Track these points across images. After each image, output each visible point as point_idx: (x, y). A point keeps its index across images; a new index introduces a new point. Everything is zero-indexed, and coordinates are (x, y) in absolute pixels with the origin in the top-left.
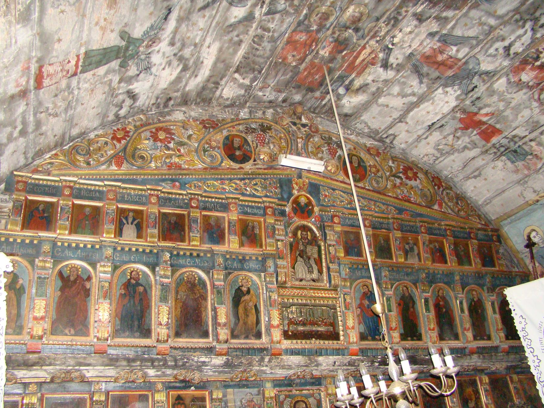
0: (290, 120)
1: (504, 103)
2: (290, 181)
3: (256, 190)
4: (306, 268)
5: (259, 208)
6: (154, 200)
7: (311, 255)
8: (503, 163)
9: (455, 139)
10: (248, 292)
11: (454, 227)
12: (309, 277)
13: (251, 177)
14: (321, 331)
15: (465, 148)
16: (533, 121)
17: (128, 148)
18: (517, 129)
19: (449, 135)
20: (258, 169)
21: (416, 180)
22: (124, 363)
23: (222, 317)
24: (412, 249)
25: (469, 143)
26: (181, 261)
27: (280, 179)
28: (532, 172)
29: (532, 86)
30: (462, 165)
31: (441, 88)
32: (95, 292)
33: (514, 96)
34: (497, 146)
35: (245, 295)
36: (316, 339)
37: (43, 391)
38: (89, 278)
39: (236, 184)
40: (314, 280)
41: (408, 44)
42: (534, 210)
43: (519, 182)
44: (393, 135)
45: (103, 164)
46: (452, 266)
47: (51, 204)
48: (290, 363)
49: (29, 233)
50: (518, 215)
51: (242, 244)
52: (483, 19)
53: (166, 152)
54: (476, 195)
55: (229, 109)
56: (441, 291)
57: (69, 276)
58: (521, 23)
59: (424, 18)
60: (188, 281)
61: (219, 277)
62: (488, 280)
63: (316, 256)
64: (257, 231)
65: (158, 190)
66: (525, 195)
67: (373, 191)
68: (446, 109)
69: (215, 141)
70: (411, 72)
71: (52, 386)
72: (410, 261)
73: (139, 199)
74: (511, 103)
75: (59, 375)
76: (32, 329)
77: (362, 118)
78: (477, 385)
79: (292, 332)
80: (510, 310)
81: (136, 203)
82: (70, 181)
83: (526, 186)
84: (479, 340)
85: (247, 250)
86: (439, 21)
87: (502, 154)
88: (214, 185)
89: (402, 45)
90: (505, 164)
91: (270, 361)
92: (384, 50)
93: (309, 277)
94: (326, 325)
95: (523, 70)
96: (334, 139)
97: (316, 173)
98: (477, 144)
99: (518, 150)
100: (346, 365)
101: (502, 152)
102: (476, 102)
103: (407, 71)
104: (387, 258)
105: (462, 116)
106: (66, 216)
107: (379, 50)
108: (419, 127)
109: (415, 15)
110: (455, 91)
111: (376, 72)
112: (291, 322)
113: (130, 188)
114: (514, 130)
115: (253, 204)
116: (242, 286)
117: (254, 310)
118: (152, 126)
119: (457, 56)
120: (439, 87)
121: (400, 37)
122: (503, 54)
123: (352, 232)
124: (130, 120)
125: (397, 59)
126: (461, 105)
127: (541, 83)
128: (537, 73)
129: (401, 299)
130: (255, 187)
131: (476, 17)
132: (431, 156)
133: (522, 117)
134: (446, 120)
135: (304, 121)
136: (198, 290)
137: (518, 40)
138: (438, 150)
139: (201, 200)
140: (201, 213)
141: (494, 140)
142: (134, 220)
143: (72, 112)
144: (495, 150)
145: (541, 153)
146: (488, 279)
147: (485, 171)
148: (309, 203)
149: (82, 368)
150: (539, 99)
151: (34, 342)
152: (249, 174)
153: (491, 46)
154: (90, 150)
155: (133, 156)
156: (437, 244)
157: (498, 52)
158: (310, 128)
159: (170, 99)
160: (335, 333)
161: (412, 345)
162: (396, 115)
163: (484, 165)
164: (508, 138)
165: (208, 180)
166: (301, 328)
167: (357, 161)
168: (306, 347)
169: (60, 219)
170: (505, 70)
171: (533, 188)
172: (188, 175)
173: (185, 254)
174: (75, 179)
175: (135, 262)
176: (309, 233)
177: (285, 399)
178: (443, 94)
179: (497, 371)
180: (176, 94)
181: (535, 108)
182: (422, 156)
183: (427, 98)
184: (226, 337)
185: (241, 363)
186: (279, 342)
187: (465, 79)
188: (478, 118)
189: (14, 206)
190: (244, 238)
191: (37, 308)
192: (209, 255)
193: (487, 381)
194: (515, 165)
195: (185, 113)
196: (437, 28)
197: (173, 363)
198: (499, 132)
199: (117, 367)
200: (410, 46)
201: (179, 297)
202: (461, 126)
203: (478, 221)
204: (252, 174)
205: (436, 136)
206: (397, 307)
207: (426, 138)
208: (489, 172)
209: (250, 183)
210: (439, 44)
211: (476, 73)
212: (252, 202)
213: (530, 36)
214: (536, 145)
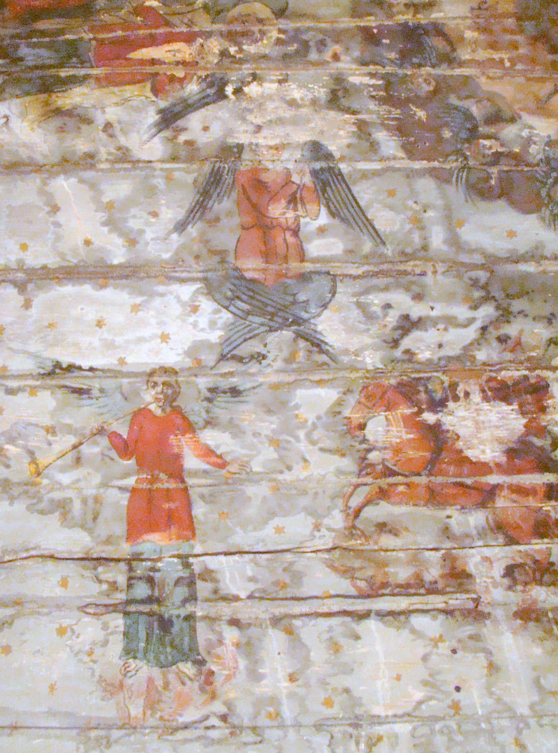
8: (100, 635)
9: (70, 458)
16: (291, 563)
18: (236, 557)
25: (85, 502)
29: (371, 465)
31: (198, 285)
33: (315, 456)
34: (140, 569)
41: (259, 121)
52: (431, 214)
58: (477, 294)
59: (345, 102)
70: (195, 181)
74: (289, 468)
86: (360, 137)
89: (250, 111)
90: (105, 643)
92: (211, 85)
95: (389, 407)
98: (101, 518)
103: (188, 172)
105: (153, 407)
107: (203, 74)
108: (34, 347)
109: (339, 79)
110: (212, 324)
111: (138, 110)
114: (226, 554)
119: (310, 241)
120: (193, 280)
121: (267, 92)
122: (387, 330)
125: (206, 129)
127: (398, 474)
128: (409, 440)
131: (423, 199)
133: (279, 530)
134: (109, 384)
137: (441, 326)
145: (228, 678)
147: (32, 621)
150: (357, 513)
153: (386, 289)
157: (386, 315)
164: (187, 565)
170: (354, 375)
178: (183, 304)
181: (329, 529)
187: (263, 315)
194: (126, 666)
196: (339, 148)
200: (259, 128)
210: (308, 180)
211: (298, 321)
213: (468, 342)
214: (237, 645)
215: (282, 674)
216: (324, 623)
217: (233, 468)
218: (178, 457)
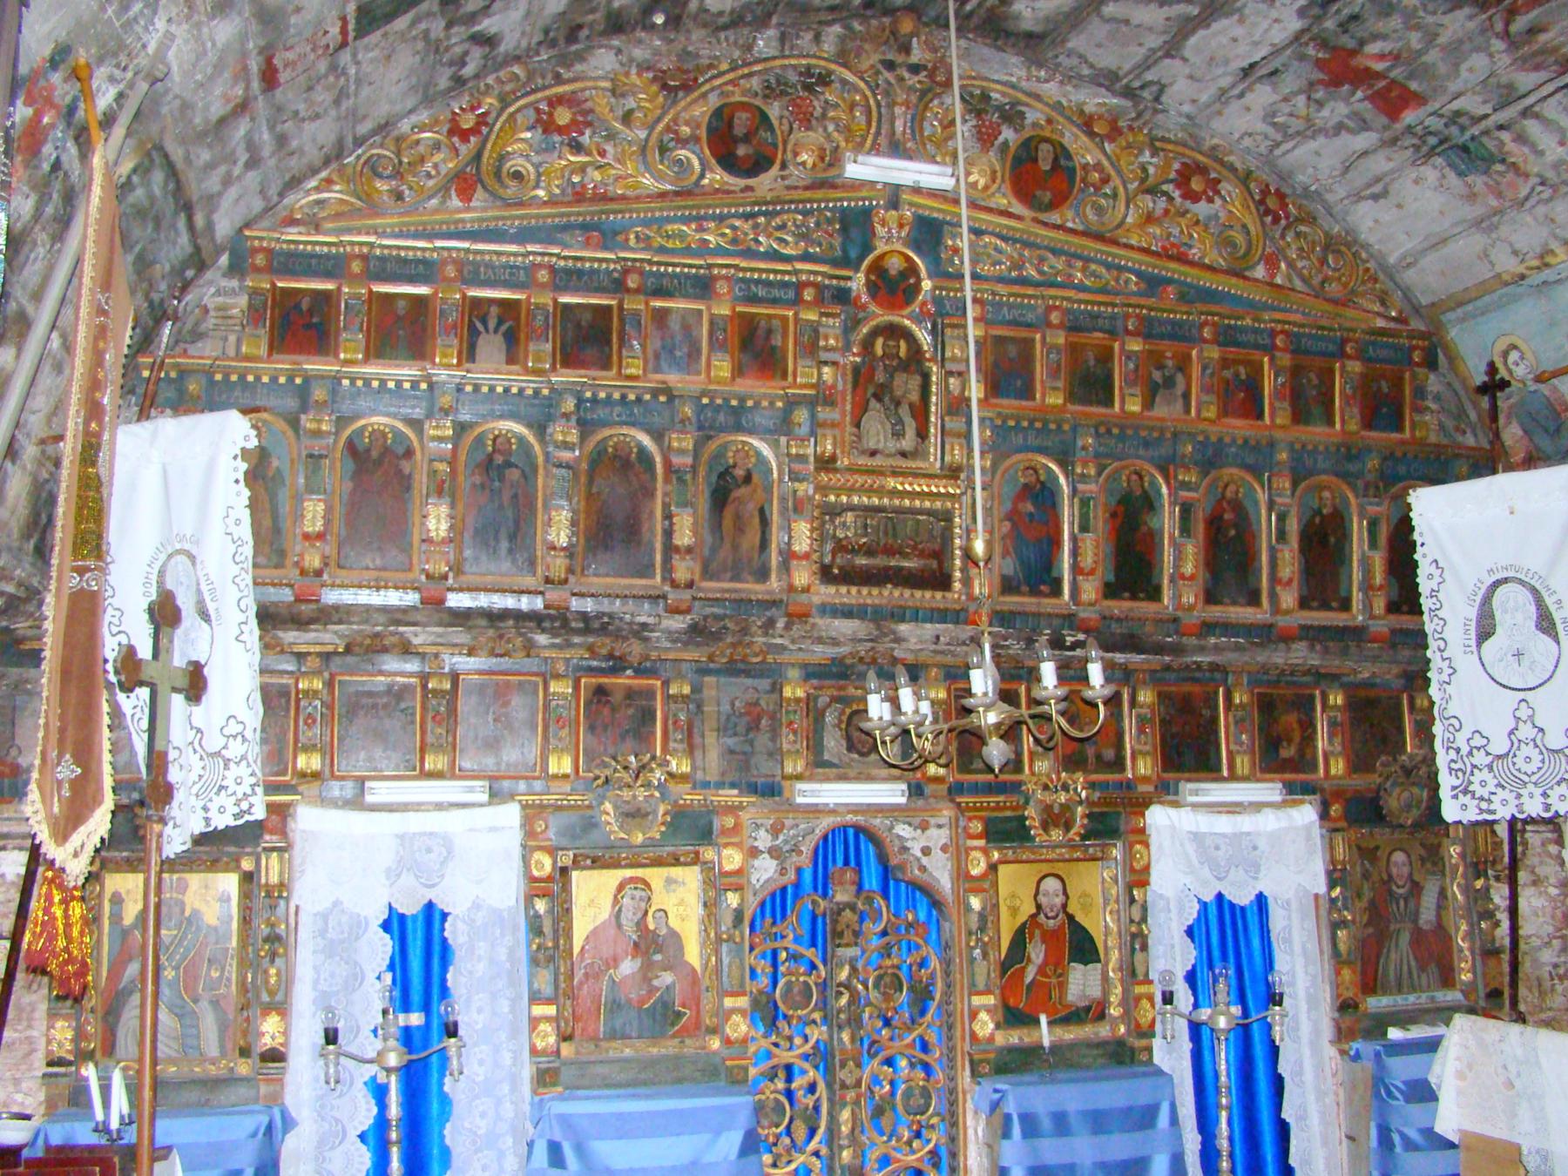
0: (875, 58)
1: (1419, 35)
2: (866, 214)
3: (782, 241)
4: (888, 426)
5: (785, 285)
6: (543, 276)
7: (904, 396)
8: (1437, 174)
10: (748, 479)
11: (1302, 326)
12: (892, 445)
13: (772, 208)
14: (909, 569)
15: (1340, 128)
17: (486, 154)
19: (1295, 94)
20: (788, 188)
21: (1210, 200)
22: (483, 622)
23: (683, 535)
24: (1169, 383)
26: (602, 413)
27: (843, 211)
28: (1507, 204)
30: (1339, 166)
32: (421, 481)
35: (739, 486)
36: (896, 585)
37: (333, 669)
38: (409, 453)
39: (734, 228)
40: (904, 454)
42: (1516, 298)
43: (1477, 223)
44: (1158, 82)
45: (430, 198)
46: (1273, 426)
47: (326, 295)
48: (834, 634)
49: (283, 364)
50: (1479, 303)
51: (738, 371)
53: (572, 158)
54: (1380, 241)
55: (731, 34)
56: (1232, 488)
57: (368, 450)
60: (615, 456)
61: (684, 444)
62: (1369, 465)
63: (915, 397)
64: (777, 341)
65: (551, 255)
66: (1493, 258)
67: (1084, 234)
68: (1279, 35)
69: (687, 123)
71: (350, 659)
72: (1161, 411)
73: (511, 274)
75: (359, 639)
76: (301, 555)
77: (1070, 45)
78: (1313, 709)
79: (841, 568)
80: (1414, 542)
81: (506, 285)
82: (361, 244)
83: (1494, 236)
84: (1318, 609)
85: (755, 387)
87: (1432, 152)
88: (682, 236)
90: (1444, 176)
91: (788, 627)
93: (892, 445)
94: (922, 555)
96: (994, 95)
97: (933, 194)
99: (1472, 146)
100: (964, 643)
101: (1433, 148)
102: (1352, 26)
104: (1099, 403)
106: (358, 320)
112: (841, 547)
113: (489, 252)
115: (772, 277)
116: (734, 466)
117: (756, 520)
118: (539, 95)
123: (1013, 339)
124: (490, 80)
126: (1315, 30)
129: (1119, 502)
130: (778, 234)
132: (1259, 138)
135: (917, 55)
136: (636, 475)
138: (1274, 125)
139: (651, 272)
140: (647, 304)
141: (1409, 117)
142: (500, 323)
143: (351, 101)
144: (1415, 141)
146: (1372, 463)
147: (1396, 185)
148: (912, 270)
149: (401, 629)
151: (307, 581)
152: (767, 203)
154: (400, 162)
155: (498, 174)
156: (1242, 370)
158: (931, 76)
159: (580, 27)
160: (942, 574)
161: (1131, 609)
162: (1154, 41)
163: (1392, 171)
164: (1441, 116)
165: (668, 220)
166: (862, 561)
167: (1052, 156)
168: (869, 601)
169: (345, 328)
171: (1511, 245)
172: (621, 212)
173: (609, 396)
174: (372, 239)
175: (502, 417)
176: (903, 344)
177: (829, 705)
179: (1378, 680)
180: (591, 17)
182: (1237, 136)
183: (1226, 8)
184: (689, 576)
185: (725, 627)
186: (806, 590)
188: (1360, 62)
189: (250, 306)
190: (746, 358)
191: (309, 516)
192: (662, 399)
193: (1340, 701)
195: (619, 51)
197: (581, 625)
198: (1420, 100)
199: (470, 628)
201: (594, 490)
202: (1321, 76)
203: (1376, 308)
204: (777, 201)
205: (1262, 96)
206: (1105, 521)
207: (1241, 95)
208: (1405, 187)
209: (768, 223)
212: (768, 271)
215: (1553, 145)
216: (1552, 101)
217: (1405, 55)
218: (1367, 70)
